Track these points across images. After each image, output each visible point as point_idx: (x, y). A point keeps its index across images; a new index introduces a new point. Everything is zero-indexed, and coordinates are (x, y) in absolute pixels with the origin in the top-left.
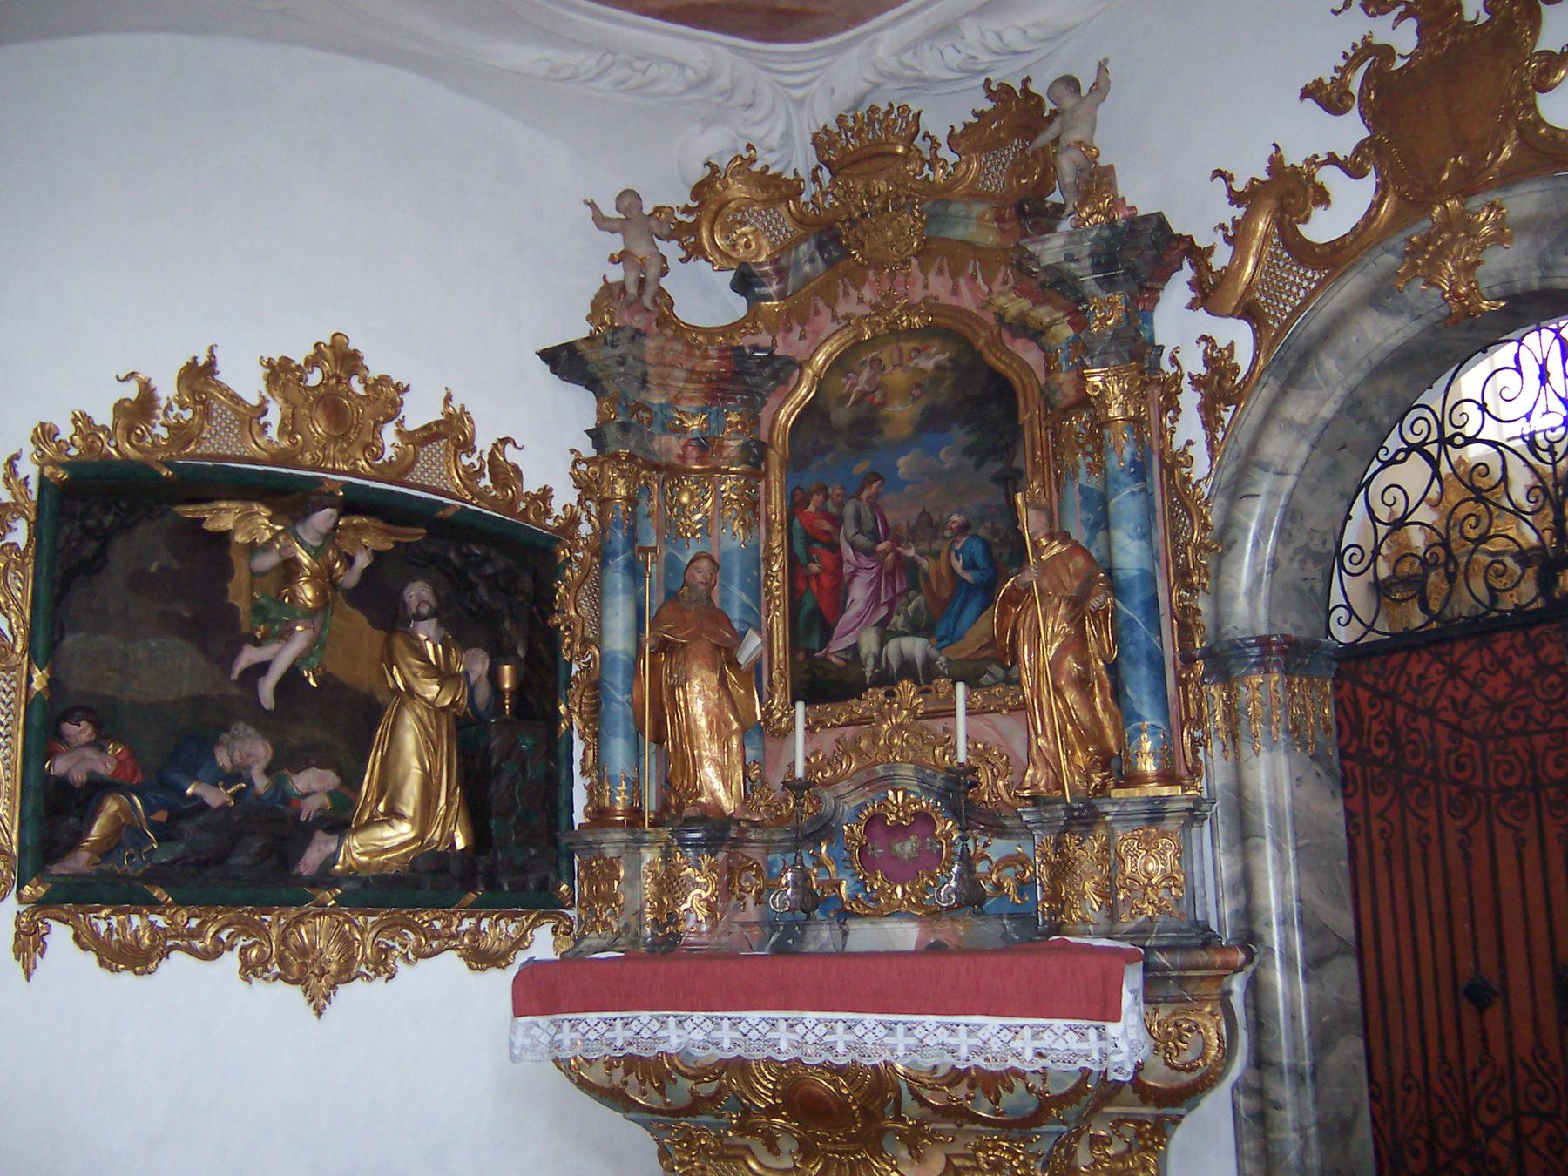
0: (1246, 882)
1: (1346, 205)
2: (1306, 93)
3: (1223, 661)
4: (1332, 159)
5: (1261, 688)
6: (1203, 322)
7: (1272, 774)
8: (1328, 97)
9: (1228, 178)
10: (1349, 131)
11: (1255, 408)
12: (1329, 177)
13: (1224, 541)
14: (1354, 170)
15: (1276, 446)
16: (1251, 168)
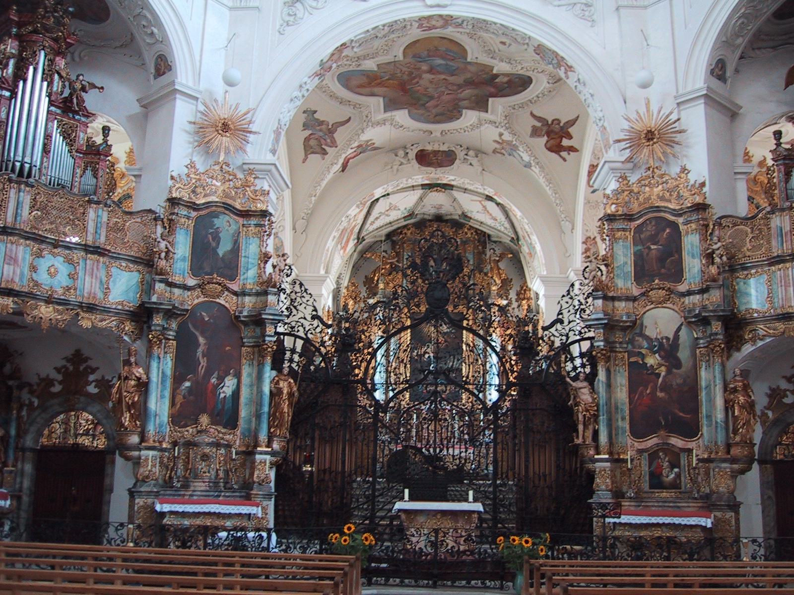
0: (21, 483)
1: (57, 388)
2: (55, 368)
3: (23, 450)
4: (56, 380)
5: (29, 454)
6: (29, 396)
7: (28, 468)
8: (58, 370)
9: (39, 376)
10: (60, 377)
11: (37, 413)
12: (56, 383)
13: (26, 432)
14: (60, 383)
15: (38, 420)
16: (43, 375)
